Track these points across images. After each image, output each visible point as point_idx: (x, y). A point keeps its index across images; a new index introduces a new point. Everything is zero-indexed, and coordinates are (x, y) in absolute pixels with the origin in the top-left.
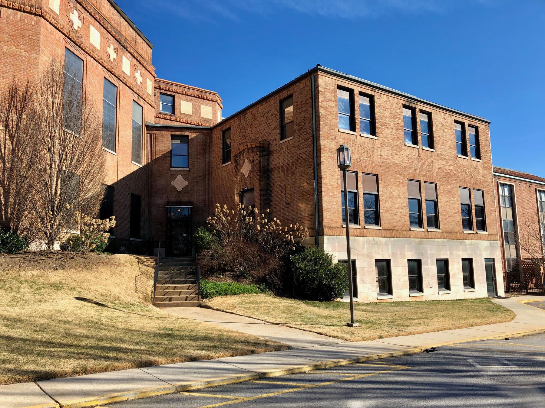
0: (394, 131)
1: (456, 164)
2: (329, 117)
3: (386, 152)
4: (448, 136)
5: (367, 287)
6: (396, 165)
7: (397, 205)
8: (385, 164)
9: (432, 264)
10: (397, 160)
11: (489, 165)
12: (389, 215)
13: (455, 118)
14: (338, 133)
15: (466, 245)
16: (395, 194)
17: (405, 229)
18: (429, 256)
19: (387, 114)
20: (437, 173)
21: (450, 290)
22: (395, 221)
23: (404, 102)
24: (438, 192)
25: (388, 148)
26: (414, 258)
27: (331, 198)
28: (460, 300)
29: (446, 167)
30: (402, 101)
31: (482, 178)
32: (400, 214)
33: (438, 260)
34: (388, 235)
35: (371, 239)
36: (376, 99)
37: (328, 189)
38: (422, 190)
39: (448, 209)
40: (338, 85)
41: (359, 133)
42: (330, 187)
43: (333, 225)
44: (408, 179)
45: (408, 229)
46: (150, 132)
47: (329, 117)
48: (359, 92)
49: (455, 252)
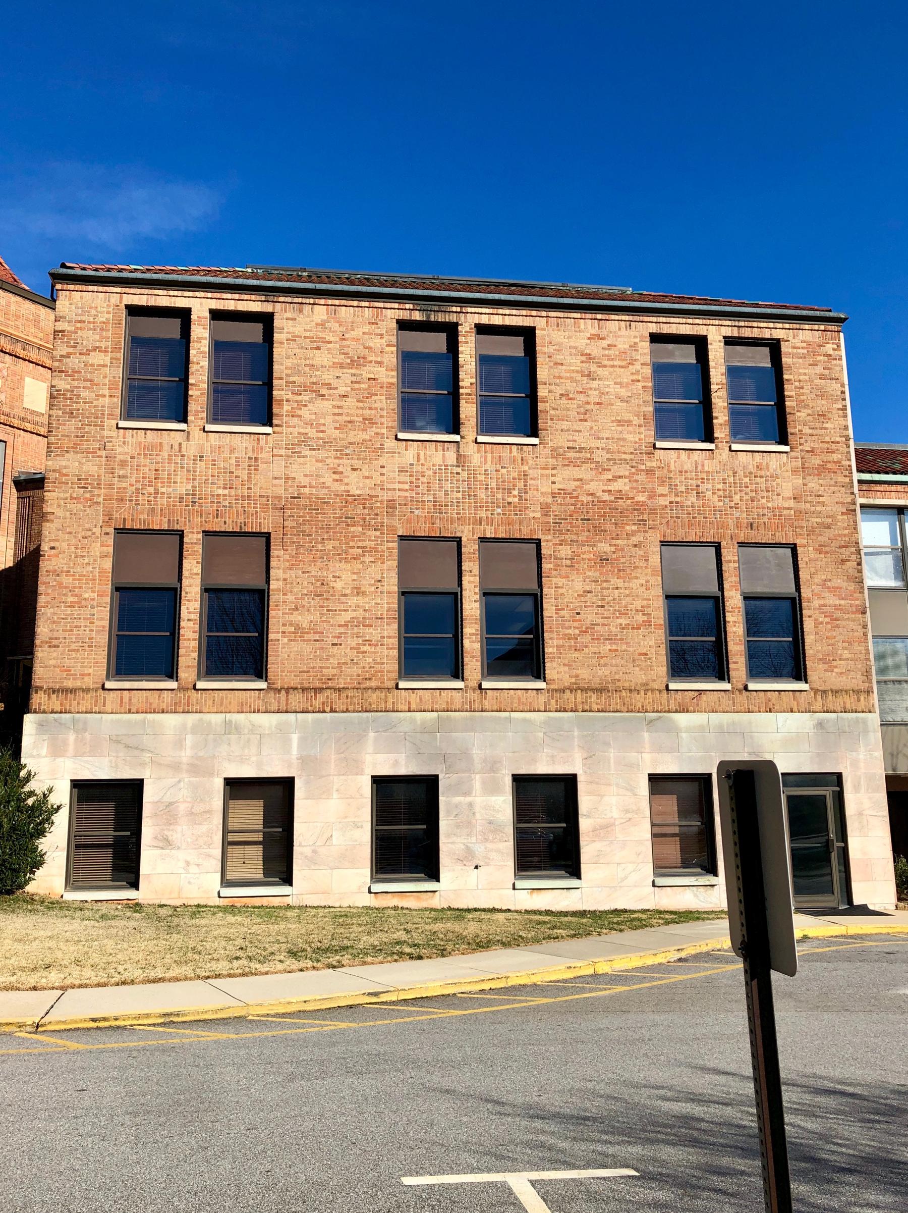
0: (351, 402)
1: (650, 472)
2: (85, 394)
3: (311, 466)
4: (613, 389)
5: (182, 857)
6: (350, 499)
7: (346, 617)
8: (303, 502)
9: (492, 788)
10: (356, 484)
11: (835, 457)
12: (307, 649)
13: (653, 328)
14: (114, 433)
15: (674, 729)
16: (339, 585)
17: (374, 684)
18: (478, 765)
19: (322, 358)
20: (546, 509)
21: (579, 878)
22: (334, 661)
23: (404, 315)
24: (546, 566)
25: (321, 454)
26: (402, 771)
27: (69, 611)
28: (616, 910)
29: (593, 487)
30: (393, 312)
31: (791, 503)
32: (353, 642)
33: (519, 780)
34: (294, 705)
35: (216, 719)
36: (277, 323)
37: (60, 584)
38: (465, 566)
39: (590, 617)
40: (127, 306)
41: (201, 423)
42: (66, 580)
43: (69, 684)
44: (402, 538)
45: (391, 684)
46: (24, 494)
47: (85, 394)
48: (211, 311)
49: (612, 754)
